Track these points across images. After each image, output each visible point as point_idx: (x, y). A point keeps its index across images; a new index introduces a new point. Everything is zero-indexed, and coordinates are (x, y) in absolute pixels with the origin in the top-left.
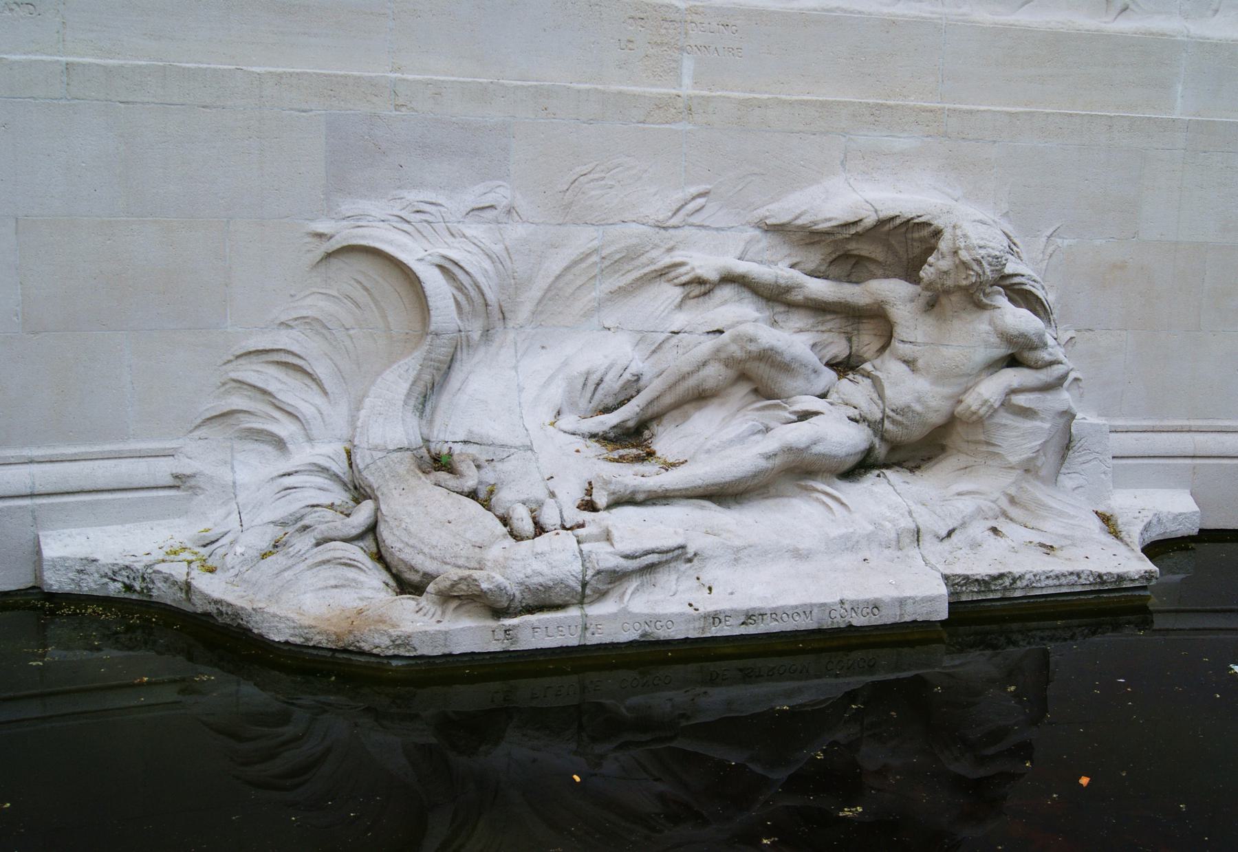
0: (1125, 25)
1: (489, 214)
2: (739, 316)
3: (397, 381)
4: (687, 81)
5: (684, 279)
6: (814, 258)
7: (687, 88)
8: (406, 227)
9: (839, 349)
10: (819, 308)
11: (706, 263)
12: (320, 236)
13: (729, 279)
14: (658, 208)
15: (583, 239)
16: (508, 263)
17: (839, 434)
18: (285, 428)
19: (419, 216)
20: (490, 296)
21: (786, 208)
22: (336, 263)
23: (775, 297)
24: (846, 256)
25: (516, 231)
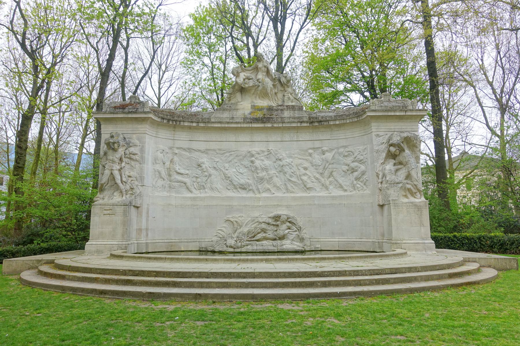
0: (309, 195)
7: (261, 204)
9: (276, 229)
10: (273, 225)
17: (271, 236)
23: (269, 224)
25: (243, 218)
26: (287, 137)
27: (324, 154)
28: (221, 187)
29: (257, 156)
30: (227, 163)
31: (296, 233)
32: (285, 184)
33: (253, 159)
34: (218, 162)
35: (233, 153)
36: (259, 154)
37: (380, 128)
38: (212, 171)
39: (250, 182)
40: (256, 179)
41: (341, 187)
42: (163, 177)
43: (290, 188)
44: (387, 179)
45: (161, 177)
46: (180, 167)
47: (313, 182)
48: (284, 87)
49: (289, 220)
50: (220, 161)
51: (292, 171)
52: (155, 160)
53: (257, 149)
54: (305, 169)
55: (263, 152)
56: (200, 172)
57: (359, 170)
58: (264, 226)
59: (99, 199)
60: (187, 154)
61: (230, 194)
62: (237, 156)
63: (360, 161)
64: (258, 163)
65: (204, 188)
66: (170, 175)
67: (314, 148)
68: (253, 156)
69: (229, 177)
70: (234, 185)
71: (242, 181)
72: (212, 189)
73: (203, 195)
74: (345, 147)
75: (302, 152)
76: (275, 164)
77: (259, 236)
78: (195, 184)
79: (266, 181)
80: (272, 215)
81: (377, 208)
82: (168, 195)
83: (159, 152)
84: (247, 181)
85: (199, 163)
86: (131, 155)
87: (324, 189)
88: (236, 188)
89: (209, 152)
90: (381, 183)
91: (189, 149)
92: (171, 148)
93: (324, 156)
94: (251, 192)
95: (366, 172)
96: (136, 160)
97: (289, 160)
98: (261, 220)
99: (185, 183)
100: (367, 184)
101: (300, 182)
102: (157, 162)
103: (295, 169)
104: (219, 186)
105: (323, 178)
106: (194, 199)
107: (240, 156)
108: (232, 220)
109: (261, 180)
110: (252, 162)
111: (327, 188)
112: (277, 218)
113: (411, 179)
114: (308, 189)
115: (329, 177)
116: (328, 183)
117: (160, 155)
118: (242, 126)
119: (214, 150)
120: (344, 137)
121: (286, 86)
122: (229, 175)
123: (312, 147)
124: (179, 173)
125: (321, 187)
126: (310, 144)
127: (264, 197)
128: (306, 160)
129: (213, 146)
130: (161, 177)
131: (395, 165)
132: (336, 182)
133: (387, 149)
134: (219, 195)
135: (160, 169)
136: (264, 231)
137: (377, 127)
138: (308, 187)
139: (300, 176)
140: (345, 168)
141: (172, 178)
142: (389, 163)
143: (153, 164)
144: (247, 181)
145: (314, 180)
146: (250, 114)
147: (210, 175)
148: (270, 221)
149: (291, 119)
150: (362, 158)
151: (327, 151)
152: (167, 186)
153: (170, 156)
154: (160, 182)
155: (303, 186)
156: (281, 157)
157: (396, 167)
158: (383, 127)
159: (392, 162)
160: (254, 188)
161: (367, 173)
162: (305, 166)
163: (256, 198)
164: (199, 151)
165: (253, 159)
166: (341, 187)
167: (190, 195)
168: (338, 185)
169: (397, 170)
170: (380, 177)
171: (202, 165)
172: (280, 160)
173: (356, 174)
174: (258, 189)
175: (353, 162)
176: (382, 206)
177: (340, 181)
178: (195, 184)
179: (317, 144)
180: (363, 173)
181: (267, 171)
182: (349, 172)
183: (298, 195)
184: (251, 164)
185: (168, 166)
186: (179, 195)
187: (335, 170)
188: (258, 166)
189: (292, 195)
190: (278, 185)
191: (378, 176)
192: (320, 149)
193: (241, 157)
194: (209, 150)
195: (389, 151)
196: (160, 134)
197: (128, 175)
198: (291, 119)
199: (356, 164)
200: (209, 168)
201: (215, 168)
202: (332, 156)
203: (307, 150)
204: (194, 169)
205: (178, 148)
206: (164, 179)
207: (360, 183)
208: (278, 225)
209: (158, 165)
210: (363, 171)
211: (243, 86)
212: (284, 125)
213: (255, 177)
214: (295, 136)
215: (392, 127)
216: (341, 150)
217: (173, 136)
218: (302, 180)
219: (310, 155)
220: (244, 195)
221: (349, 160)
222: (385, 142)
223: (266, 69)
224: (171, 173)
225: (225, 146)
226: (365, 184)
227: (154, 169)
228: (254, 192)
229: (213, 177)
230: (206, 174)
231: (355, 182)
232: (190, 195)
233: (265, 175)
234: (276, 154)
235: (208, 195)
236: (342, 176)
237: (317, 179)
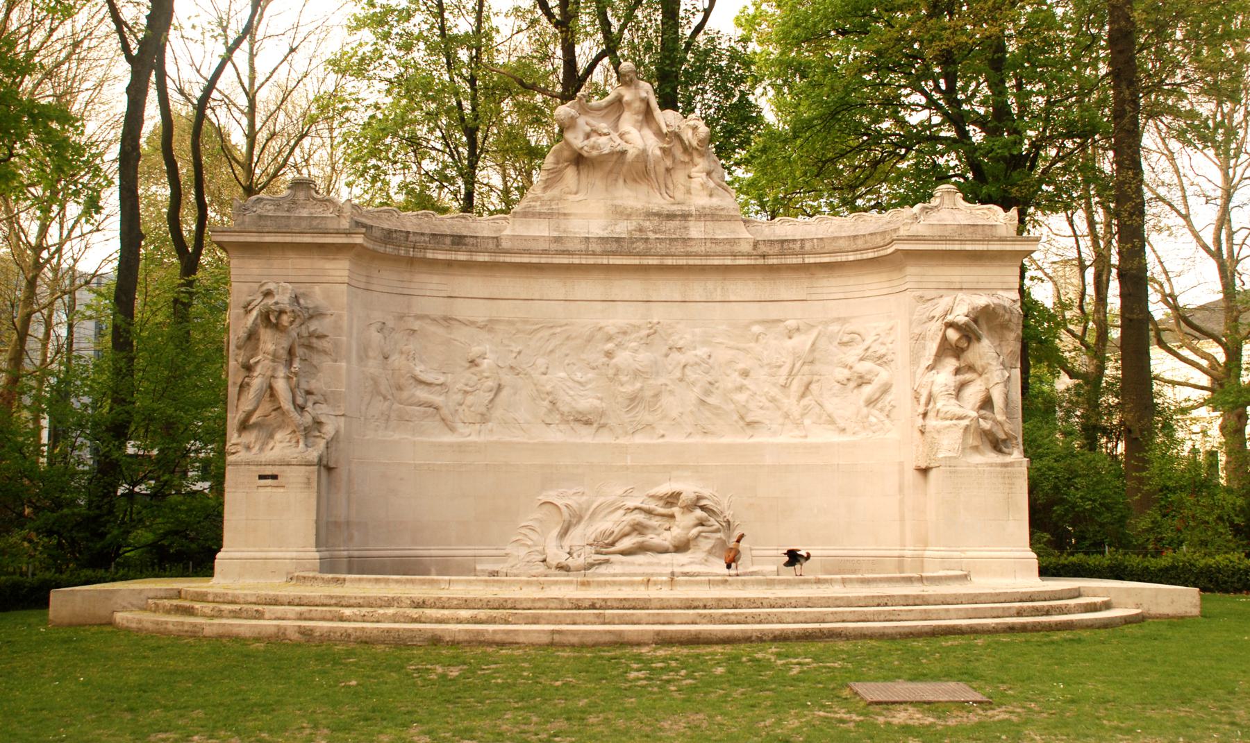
0: (752, 440)
2: (639, 517)
3: (555, 532)
6: (661, 503)
7: (629, 463)
9: (667, 526)
11: (631, 504)
13: (636, 509)
14: (620, 492)
15: (600, 500)
18: (530, 543)
21: (652, 492)
23: (649, 512)
25: (584, 498)
27: (790, 338)
31: (718, 535)
33: (610, 346)
34: (519, 353)
35: (559, 330)
36: (625, 333)
37: (925, 279)
38: (507, 378)
41: (831, 421)
42: (384, 391)
44: (939, 405)
46: (422, 367)
47: (761, 408)
48: (691, 154)
49: (703, 503)
51: (710, 379)
54: (745, 374)
55: (637, 328)
56: (476, 378)
57: (876, 379)
58: (639, 517)
59: (239, 448)
60: (440, 331)
62: (568, 338)
63: (880, 358)
70: (562, 414)
71: (586, 402)
73: (482, 439)
74: (842, 320)
77: (626, 543)
81: (911, 476)
84: (597, 402)
85: (471, 356)
86: (314, 340)
89: (497, 327)
90: (925, 415)
92: (401, 317)
93: (789, 343)
94: (605, 430)
95: (891, 386)
96: (325, 352)
97: (702, 352)
100: (892, 416)
102: (371, 354)
105: (788, 397)
106: (461, 448)
108: (559, 502)
109: (634, 400)
110: (609, 354)
111: (798, 424)
112: (672, 499)
113: (992, 407)
114: (749, 424)
115: (803, 396)
116: (796, 411)
117: (376, 337)
118: (584, 262)
119: (511, 323)
121: (695, 154)
122: (548, 388)
124: (421, 382)
125: (781, 420)
126: (754, 311)
128: (745, 350)
129: (505, 310)
130: (379, 393)
131: (958, 371)
132: (817, 409)
133: (941, 334)
136: (638, 528)
137: (918, 279)
138: (748, 420)
140: (842, 374)
142: (944, 367)
145: (768, 404)
147: (500, 388)
148: (652, 505)
149: (708, 244)
150: (883, 350)
151: (798, 329)
155: (736, 417)
156: (680, 344)
157: (961, 378)
158: (933, 279)
159: (951, 363)
160: (612, 422)
161: (893, 390)
162: (741, 366)
164: (473, 323)
165: (610, 346)
166: (831, 421)
167: (448, 438)
168: (824, 417)
169: (961, 387)
170: (923, 400)
171: (478, 361)
173: (867, 390)
175: (861, 359)
176: (924, 471)
177: (831, 405)
179: (773, 311)
180: (886, 389)
182: (852, 385)
187: (816, 378)
189: (710, 440)
190: (674, 414)
191: (917, 399)
192: (782, 325)
194: (498, 321)
195: (944, 338)
197: (306, 388)
198: (708, 244)
199: (867, 366)
202: (810, 343)
205: (418, 317)
207: (876, 412)
208: (672, 516)
210: (886, 384)
211: (585, 154)
214: (719, 290)
215: (958, 279)
216: (834, 328)
220: (588, 440)
221: (852, 354)
222: (938, 316)
223: (643, 106)
226: (888, 416)
230: (490, 383)
231: (865, 410)
232: (448, 438)
233: (642, 389)
234: (670, 335)
235: (495, 438)
236: (835, 395)
237: (773, 400)
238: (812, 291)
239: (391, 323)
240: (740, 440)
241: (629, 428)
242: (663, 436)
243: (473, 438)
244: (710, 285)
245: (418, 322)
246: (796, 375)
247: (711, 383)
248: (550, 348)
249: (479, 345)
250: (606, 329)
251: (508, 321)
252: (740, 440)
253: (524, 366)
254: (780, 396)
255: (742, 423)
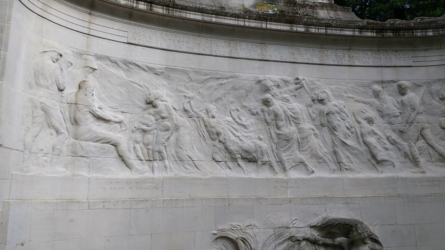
1: (250, 227)
4: (289, 194)
5: (294, 240)
7: (290, 197)
8: (233, 231)
12: (214, 234)
16: (255, 238)
19: (235, 228)
20: (252, 246)
22: (218, 240)
24: (330, 233)
26: (331, 56)
27: (403, 94)
28: (201, 156)
29: (275, 90)
30: (211, 102)
32: (335, 152)
33: (268, 96)
34: (192, 98)
35: (225, 81)
36: (278, 86)
39: (265, 145)
40: (276, 141)
42: (57, 125)
43: (344, 160)
45: (51, 126)
46: (102, 104)
47: (387, 149)
50: (198, 97)
52: (36, 76)
53: (277, 78)
56: (153, 118)
60: (121, 73)
61: (222, 172)
62: (234, 88)
64: (277, 105)
65: (162, 159)
66: (76, 122)
67: (382, 82)
68: (267, 90)
69: (218, 134)
72: (180, 160)
73: (158, 175)
75: (361, 89)
76: (310, 110)
78: (138, 146)
79: (295, 146)
80: (316, 220)
82: (68, 173)
83: (47, 56)
87: (410, 164)
88: (234, 160)
89: (172, 75)
91: (127, 63)
92: (80, 55)
93: (404, 98)
94: (266, 167)
98: (299, 235)
99: (115, 145)
101: (363, 148)
102: (42, 82)
103: (351, 121)
104: (197, 155)
107: (240, 88)
110: (266, 103)
111: (415, 162)
114: (378, 162)
118: (247, 24)
120: (440, 63)
123: (379, 79)
125: (402, 159)
127: (296, 180)
130: (51, 126)
134: (194, 174)
135: (49, 103)
138: (379, 158)
139: (362, 135)
141: (82, 129)
143: (31, 87)
144: (259, 142)
145: (389, 145)
146: (255, 6)
147: (177, 128)
148: (315, 234)
152: (64, 149)
153: (79, 74)
154: (47, 140)
155: (369, 157)
156: (322, 96)
160: (273, 160)
163: (278, 181)
165: (268, 96)
171: (158, 102)
172: (321, 101)
174: (281, 162)
178: (138, 146)
179: (388, 74)
181: (297, 124)
183: (360, 176)
184: (264, 107)
185: (72, 99)
186: (100, 175)
188: (280, 112)
192: (395, 85)
193: (242, 91)
196: (53, 12)
200: (173, 112)
201: (186, 111)
203: (369, 86)
204: (138, 110)
205: (99, 57)
206: (57, 132)
209: (42, 92)
212: (329, 32)
213: (274, 135)
217: (86, 25)
218: (366, 143)
219: (377, 95)
220: (253, 175)
224: (79, 115)
225: (208, 63)
227: (31, 100)
228: (271, 166)
229: (182, 131)
230: (167, 123)
237: (394, 143)
238: (416, 59)
239: (69, 57)
240: (373, 175)
241: (287, 166)
242: (313, 172)
243: (149, 175)
244: (340, 53)
245: (99, 62)
246: (412, 122)
247: (348, 128)
248: (219, 95)
249: (157, 88)
250: (264, 82)
251: (183, 71)
252: (373, 175)
253: (197, 110)
254: (399, 140)
255: (374, 162)
